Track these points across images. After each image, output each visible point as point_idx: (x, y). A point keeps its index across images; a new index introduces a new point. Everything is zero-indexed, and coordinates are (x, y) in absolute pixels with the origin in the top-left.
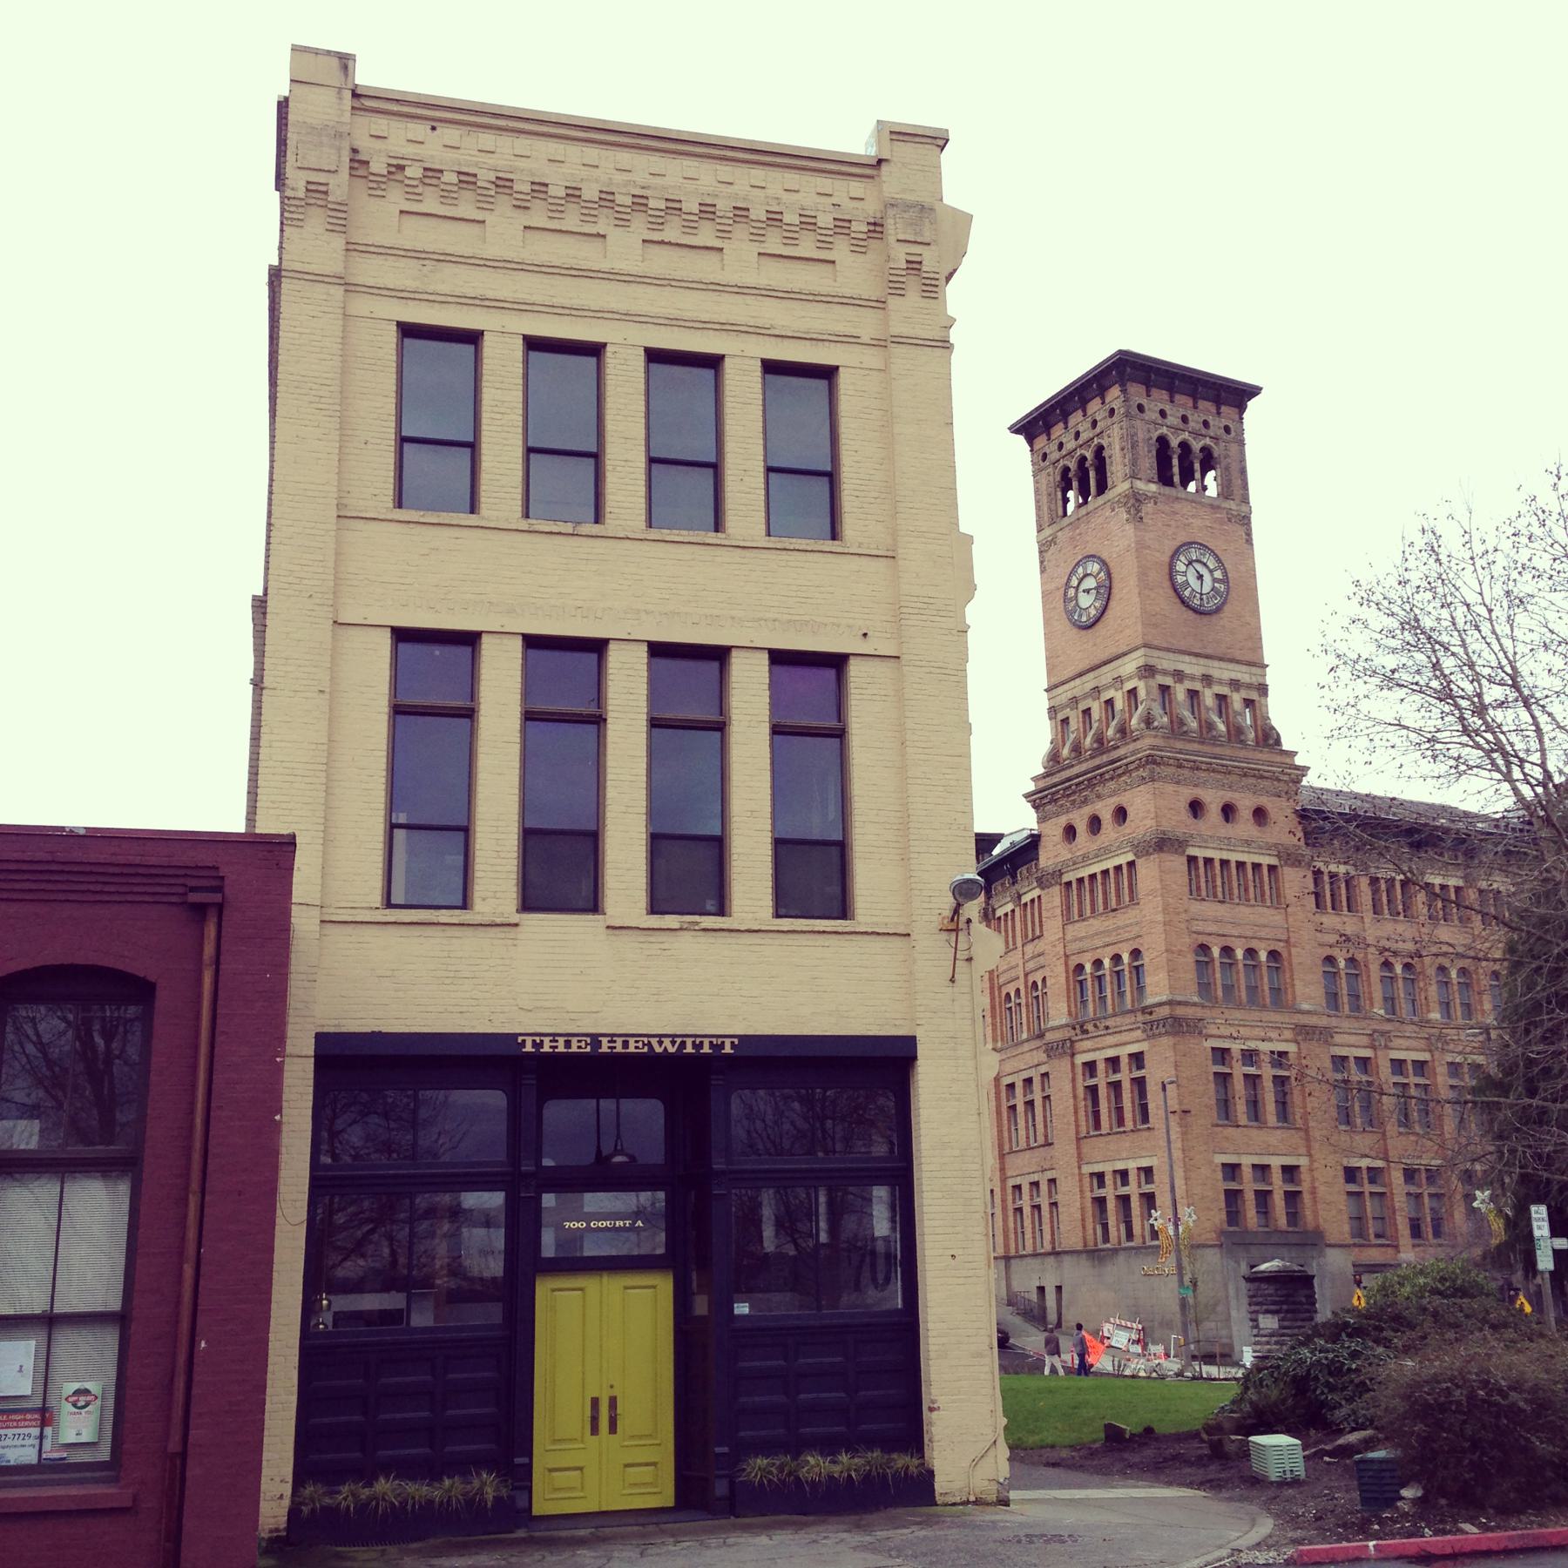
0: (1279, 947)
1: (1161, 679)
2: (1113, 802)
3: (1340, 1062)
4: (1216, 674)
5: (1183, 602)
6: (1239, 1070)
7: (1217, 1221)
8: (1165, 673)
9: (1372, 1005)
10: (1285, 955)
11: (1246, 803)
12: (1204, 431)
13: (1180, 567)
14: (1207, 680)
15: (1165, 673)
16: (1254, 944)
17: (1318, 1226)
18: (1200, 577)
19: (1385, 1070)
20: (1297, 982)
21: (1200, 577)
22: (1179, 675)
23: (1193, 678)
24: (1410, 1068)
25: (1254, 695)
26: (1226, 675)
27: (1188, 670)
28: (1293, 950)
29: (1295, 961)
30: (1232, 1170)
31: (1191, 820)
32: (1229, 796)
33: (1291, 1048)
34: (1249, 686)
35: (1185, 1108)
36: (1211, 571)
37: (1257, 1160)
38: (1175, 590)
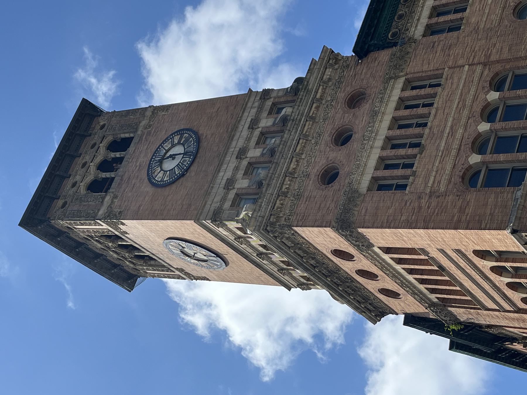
0: (488, 74)
1: (227, 205)
2: (336, 260)
4: (241, 144)
5: (183, 175)
8: (224, 199)
10: (498, 68)
11: (339, 116)
12: (96, 147)
13: (159, 176)
14: (242, 153)
15: (224, 199)
16: (478, 108)
18: (173, 157)
21: (173, 157)
22: (230, 183)
23: (237, 169)
25: (269, 103)
26: (245, 133)
27: (229, 174)
28: (493, 58)
29: (506, 55)
31: (336, 185)
32: (327, 137)
34: (260, 109)
36: (173, 146)
38: (173, 182)
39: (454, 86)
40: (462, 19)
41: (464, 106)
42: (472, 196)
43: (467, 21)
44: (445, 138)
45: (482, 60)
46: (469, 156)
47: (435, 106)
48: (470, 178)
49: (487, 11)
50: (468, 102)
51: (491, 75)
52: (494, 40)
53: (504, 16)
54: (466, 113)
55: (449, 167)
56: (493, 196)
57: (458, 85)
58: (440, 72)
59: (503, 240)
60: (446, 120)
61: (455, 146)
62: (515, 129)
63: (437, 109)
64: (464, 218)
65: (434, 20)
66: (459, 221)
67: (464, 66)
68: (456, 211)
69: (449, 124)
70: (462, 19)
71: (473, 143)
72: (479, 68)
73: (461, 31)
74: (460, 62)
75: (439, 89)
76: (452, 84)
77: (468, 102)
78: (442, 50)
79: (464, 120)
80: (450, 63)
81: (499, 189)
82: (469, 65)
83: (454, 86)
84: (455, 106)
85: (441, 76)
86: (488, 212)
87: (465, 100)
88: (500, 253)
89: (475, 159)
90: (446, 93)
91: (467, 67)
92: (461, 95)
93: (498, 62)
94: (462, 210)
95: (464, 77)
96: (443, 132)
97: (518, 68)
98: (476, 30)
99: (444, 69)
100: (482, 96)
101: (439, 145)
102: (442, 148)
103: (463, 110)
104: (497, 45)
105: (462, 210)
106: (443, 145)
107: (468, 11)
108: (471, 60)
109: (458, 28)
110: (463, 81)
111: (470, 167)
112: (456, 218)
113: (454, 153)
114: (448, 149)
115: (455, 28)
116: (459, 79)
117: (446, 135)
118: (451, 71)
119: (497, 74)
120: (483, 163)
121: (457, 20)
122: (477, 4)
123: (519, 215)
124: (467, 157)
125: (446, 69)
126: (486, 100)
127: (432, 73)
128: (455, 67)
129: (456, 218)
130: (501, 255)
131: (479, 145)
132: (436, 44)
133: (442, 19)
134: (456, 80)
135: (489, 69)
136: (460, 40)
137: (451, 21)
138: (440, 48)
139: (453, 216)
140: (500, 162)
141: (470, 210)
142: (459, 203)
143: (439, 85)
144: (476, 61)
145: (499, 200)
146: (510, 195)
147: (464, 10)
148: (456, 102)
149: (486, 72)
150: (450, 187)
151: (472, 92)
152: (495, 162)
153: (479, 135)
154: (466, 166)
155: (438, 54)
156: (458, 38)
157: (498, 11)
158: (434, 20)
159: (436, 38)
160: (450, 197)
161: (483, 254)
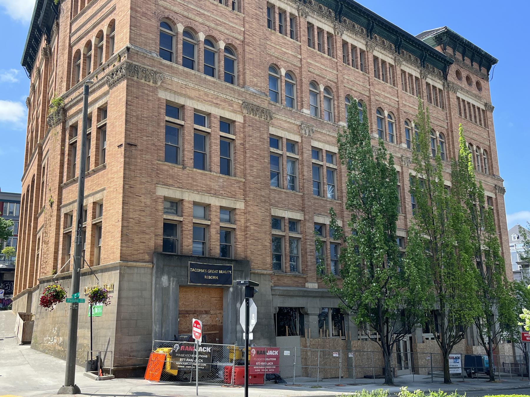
0: (236, 43)
3: (275, 141)
6: (189, 124)
7: (152, 244)
9: (302, 107)
10: (240, 50)
16: (215, 34)
17: (246, 257)
19: (307, 153)
20: (248, 72)
24: (324, 154)
28: (247, 48)
29: (248, 56)
30: (175, 205)
33: (239, 119)
35: (133, 142)
37: (197, 198)
39: (231, 19)
40: (275, 30)
41: (217, 24)
42: (155, 23)
43: (273, 33)
44: (196, 9)
45: (246, 40)
46: (183, 24)
47: (220, 4)
48: (167, 23)
49: (277, 47)
50: (219, 28)
51: (236, 45)
52: (258, 49)
53: (273, 57)
54: (213, 25)
55: (176, 9)
56: (154, 37)
57: (232, 22)
58: (242, 11)
59: (122, 40)
60: (208, 11)
61: (191, 15)
62: (199, 56)
63: (217, 6)
64: (139, 15)
65: (277, 11)
66: (136, 11)
67: (244, 27)
68: (144, 10)
69: (206, 13)
70: (275, 30)
71: (191, 28)
72: (241, 38)
73: (267, 28)
74: (247, 26)
75: (230, 9)
76: (233, 18)
77: (219, 28)
78: (256, 14)
79: (208, 23)
80: (247, 18)
81: (158, 42)
82: (244, 31)
83: (231, 19)
84: (218, 18)
85: (239, 11)
86: (143, 33)
87: (221, 25)
88: (113, 38)
89: (180, 28)
90: (227, 13)
91: (243, 30)
92: (225, 23)
93: (244, 50)
94: (144, 14)
95: (237, 27)
96: (201, 7)
97: (238, 63)
98: (266, 39)
99: (244, 14)
100: (223, 38)
101: (191, 4)
102: (189, 5)
103: (214, 24)
104: (255, 51)
105: (144, 14)
106: (192, 7)
107: (280, 34)
108: (247, 33)
109: (269, 27)
110: (234, 26)
111: (175, 24)
112: (138, 9)
113: (186, 14)
114: (188, 10)
115: (270, 24)
116: (236, 24)
117: (198, 10)
118: (242, 19)
119: (236, 49)
120: (177, 33)
121: (275, 26)
122: (283, 41)
123: (139, 53)
124: (182, 23)
125: (243, 15)
126: (220, 40)
127: (242, 5)
128: (244, 21)
129: (138, 9)
130: (111, 39)
131: (189, 32)
132: (261, 10)
133: (277, 16)
134: (236, 21)
135: (240, 44)
136: (261, 27)
137: (275, 23)
138: (258, 12)
139: (140, 8)
140: (177, 45)
141: (144, 20)
142: (149, 13)
143: (233, 9)
144: (246, 36)
145: (151, 41)
146: (154, 49)
147: (280, 32)
148: (220, 20)
149: (238, 42)
150: (162, 9)
151: (226, 31)
152: (177, 41)
153: (197, 33)
154: (176, 21)
155: (254, 10)
156: (263, 26)
157: (276, 54)
158: (277, 11)
159: (265, 10)
160: (154, 7)
161: (112, 26)
